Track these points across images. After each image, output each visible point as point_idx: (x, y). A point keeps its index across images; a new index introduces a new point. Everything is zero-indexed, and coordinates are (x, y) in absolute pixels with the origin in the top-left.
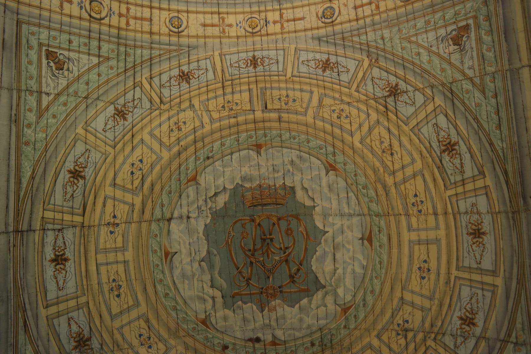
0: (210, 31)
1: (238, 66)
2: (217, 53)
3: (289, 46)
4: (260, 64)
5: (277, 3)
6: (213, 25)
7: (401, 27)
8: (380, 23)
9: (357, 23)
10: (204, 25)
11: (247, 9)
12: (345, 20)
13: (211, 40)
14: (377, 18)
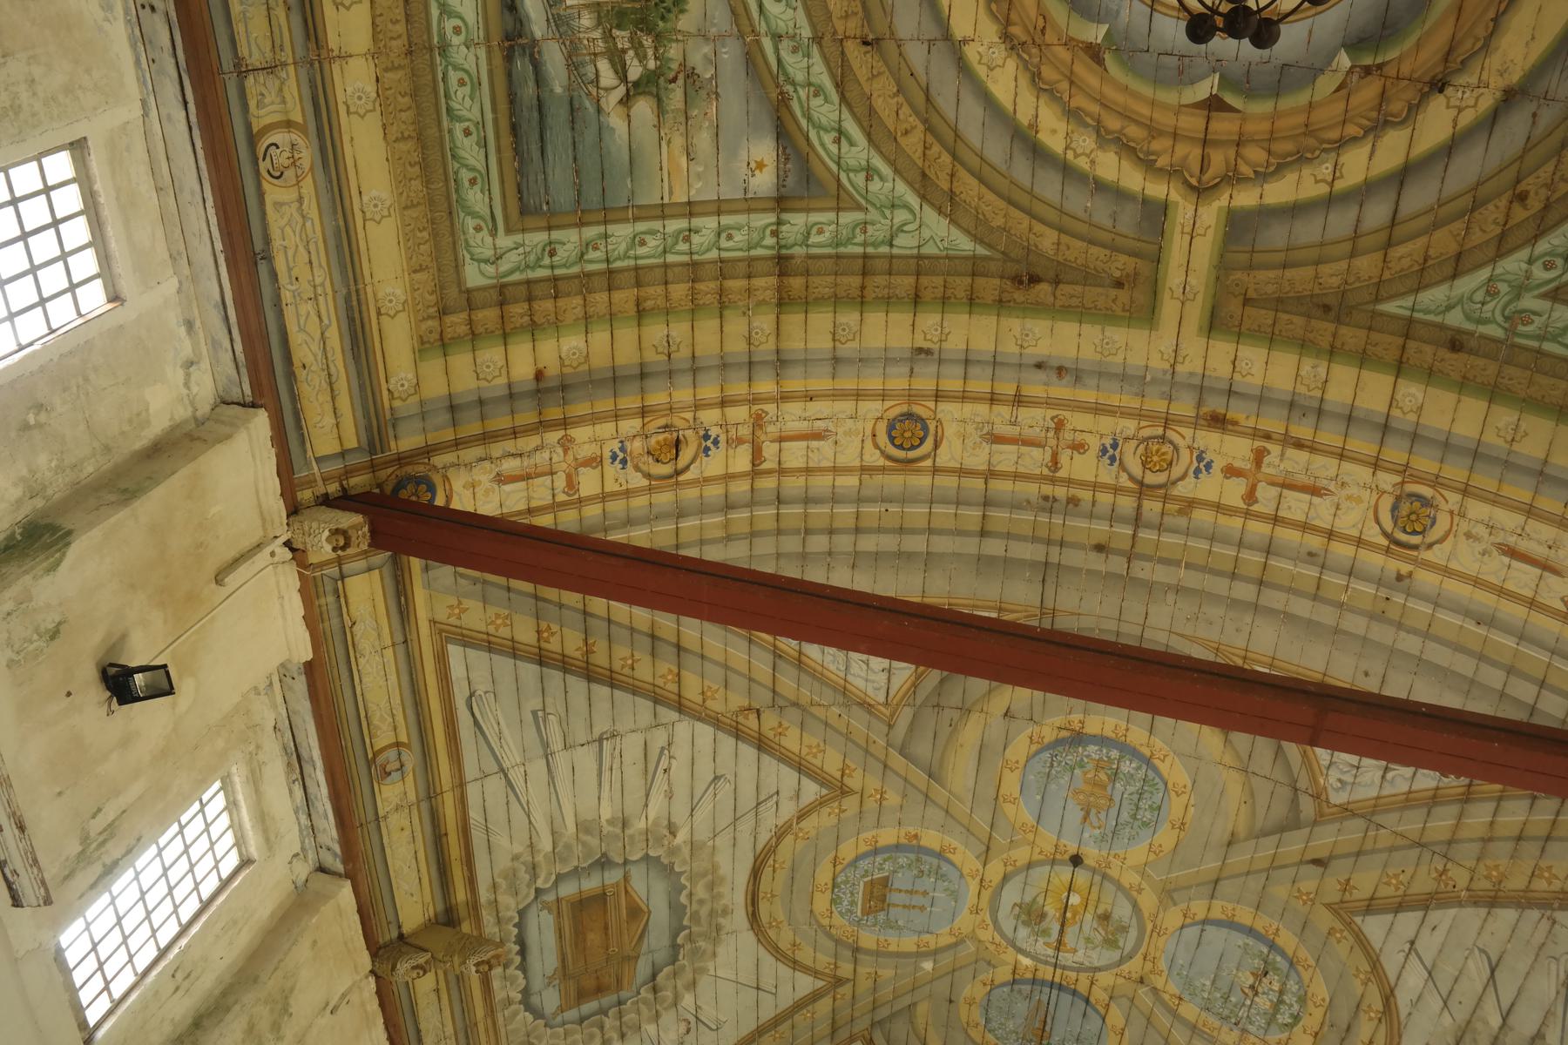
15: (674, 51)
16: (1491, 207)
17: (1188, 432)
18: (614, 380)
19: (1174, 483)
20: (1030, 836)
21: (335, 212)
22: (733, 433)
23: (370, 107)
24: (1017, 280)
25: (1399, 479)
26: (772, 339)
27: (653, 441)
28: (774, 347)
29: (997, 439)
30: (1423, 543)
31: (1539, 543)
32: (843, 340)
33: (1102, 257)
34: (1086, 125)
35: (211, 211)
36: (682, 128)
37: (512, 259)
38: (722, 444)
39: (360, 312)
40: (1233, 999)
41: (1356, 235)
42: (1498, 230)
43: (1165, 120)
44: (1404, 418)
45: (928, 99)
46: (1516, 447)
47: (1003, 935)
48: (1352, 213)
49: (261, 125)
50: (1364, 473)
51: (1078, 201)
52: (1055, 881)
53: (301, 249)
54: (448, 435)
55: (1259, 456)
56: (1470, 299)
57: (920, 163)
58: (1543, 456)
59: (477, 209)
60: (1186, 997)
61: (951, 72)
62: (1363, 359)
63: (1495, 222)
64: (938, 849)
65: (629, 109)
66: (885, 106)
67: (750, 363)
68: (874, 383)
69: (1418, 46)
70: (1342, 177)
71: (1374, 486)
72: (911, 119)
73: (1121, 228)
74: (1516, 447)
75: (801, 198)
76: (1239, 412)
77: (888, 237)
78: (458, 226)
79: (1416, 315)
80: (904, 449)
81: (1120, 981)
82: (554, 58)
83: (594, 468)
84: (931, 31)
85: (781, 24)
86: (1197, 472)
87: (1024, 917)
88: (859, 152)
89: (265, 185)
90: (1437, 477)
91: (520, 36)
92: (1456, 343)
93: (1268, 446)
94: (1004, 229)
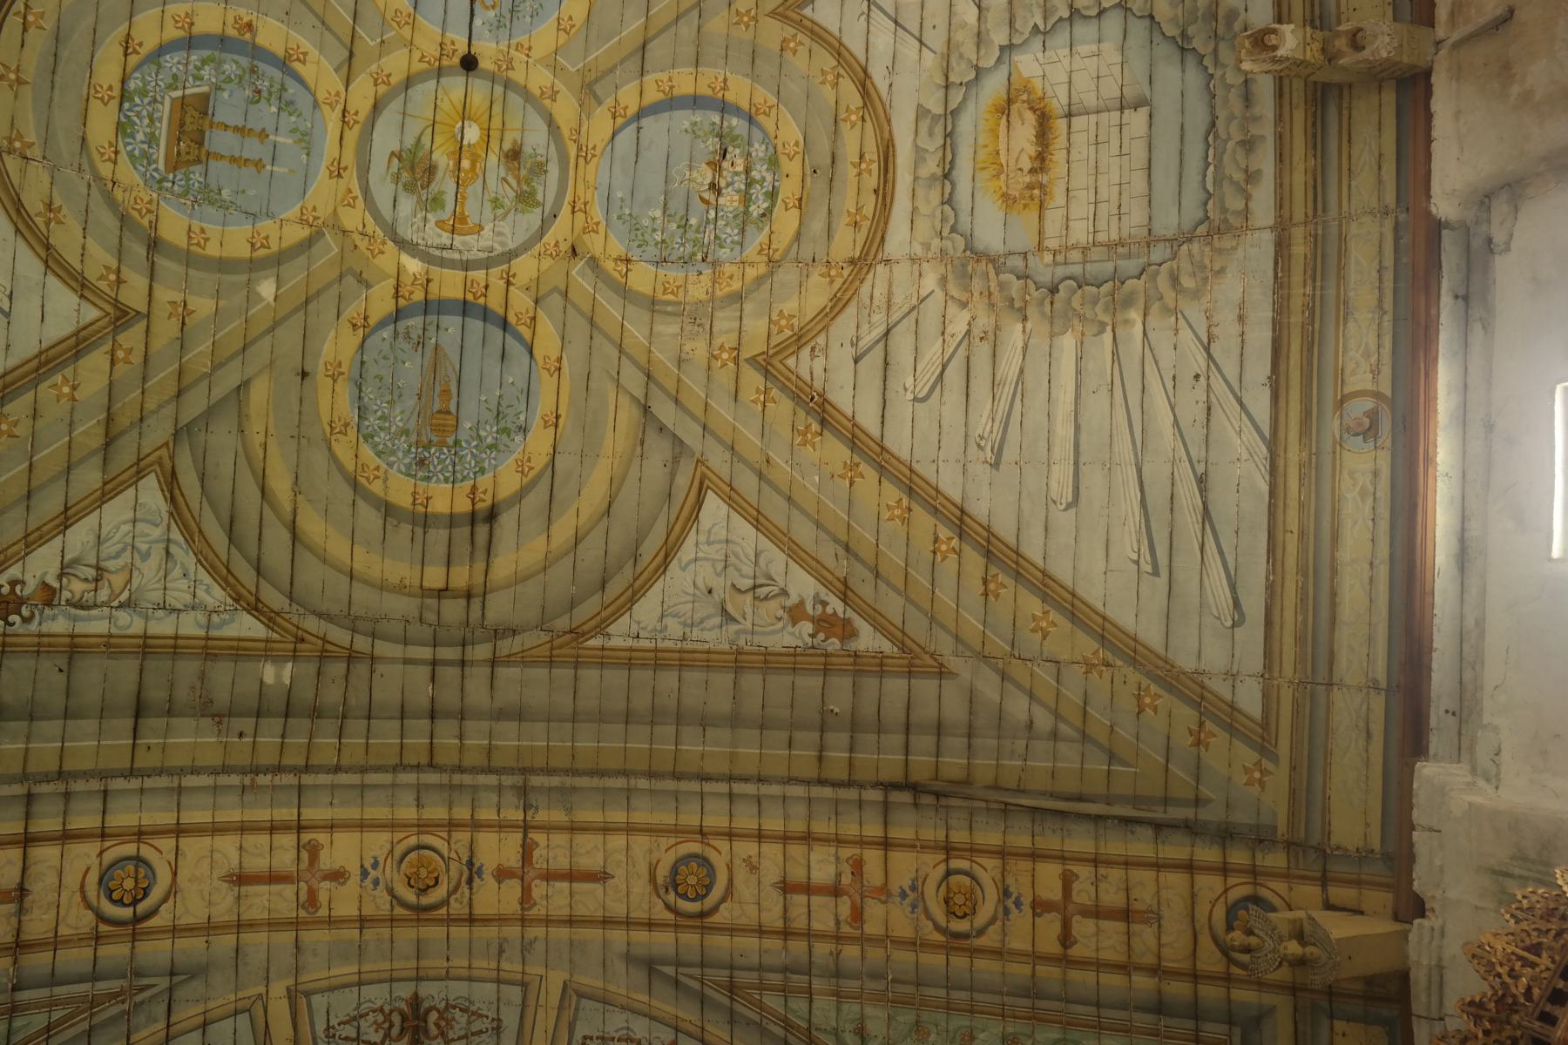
0: (262, 901)
1: (354, 1035)
2: (278, 989)
3: (541, 971)
4: (434, 1031)
5: (515, 800)
6: (273, 878)
7: (925, 1016)
8: (857, 976)
9: (785, 948)
10: (240, 879)
11: (408, 813)
12: (744, 921)
13: (261, 937)
14: (851, 952)
20: (406, 32)
40: (693, 221)
47: (377, 216)
52: (444, 105)
60: (635, 254)
64: (280, 53)
81: (547, 263)
87: (405, 176)
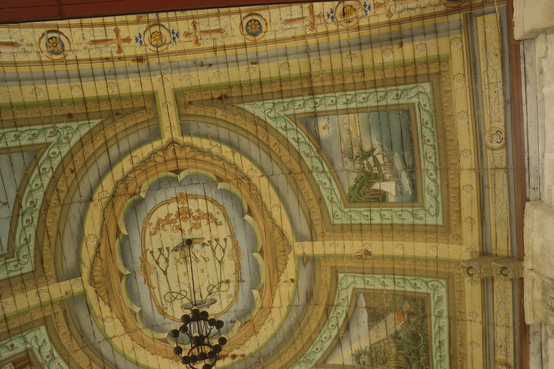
15: (358, 166)
16: (80, 165)
17: (149, 52)
18: (371, 42)
19: (147, 29)
21: (478, 116)
22: (322, 21)
23: (463, 152)
24: (226, 97)
25: (67, 58)
26: (312, 61)
27: (354, 15)
28: (310, 58)
29: (219, 31)
30: (46, 35)
31: (5, 53)
32: (285, 64)
33: (199, 111)
34: (216, 156)
35: (525, 121)
36: (353, 140)
37: (413, 93)
38: (326, 15)
39: (471, 76)
41: (117, 142)
42: (75, 159)
43: (191, 163)
44: (75, 82)
45: (270, 156)
46: (33, 87)
48: (122, 149)
49: (502, 150)
50: (80, 56)
51: (212, 130)
53: (493, 104)
54: (438, 20)
55: (120, 50)
56: (72, 134)
57: (269, 134)
58: (22, 87)
59: (425, 113)
61: (264, 166)
62: (98, 100)
63: (77, 161)
65: (372, 147)
66: (284, 152)
67: (319, 51)
68: (271, 47)
69: (123, 205)
70: (129, 160)
71: (74, 52)
72: (275, 149)
73: (195, 123)
74: (33, 87)
75: (308, 117)
76: (133, 65)
77: (275, 107)
78: (433, 107)
79: (87, 122)
80: (254, 20)
82: (398, 164)
83: (377, 3)
84: (273, 178)
85: (323, 176)
86: (140, 36)
88: (291, 136)
89: (503, 128)
90: (54, 65)
91: (410, 172)
92: (70, 117)
93: (118, 55)
94: (235, 115)
